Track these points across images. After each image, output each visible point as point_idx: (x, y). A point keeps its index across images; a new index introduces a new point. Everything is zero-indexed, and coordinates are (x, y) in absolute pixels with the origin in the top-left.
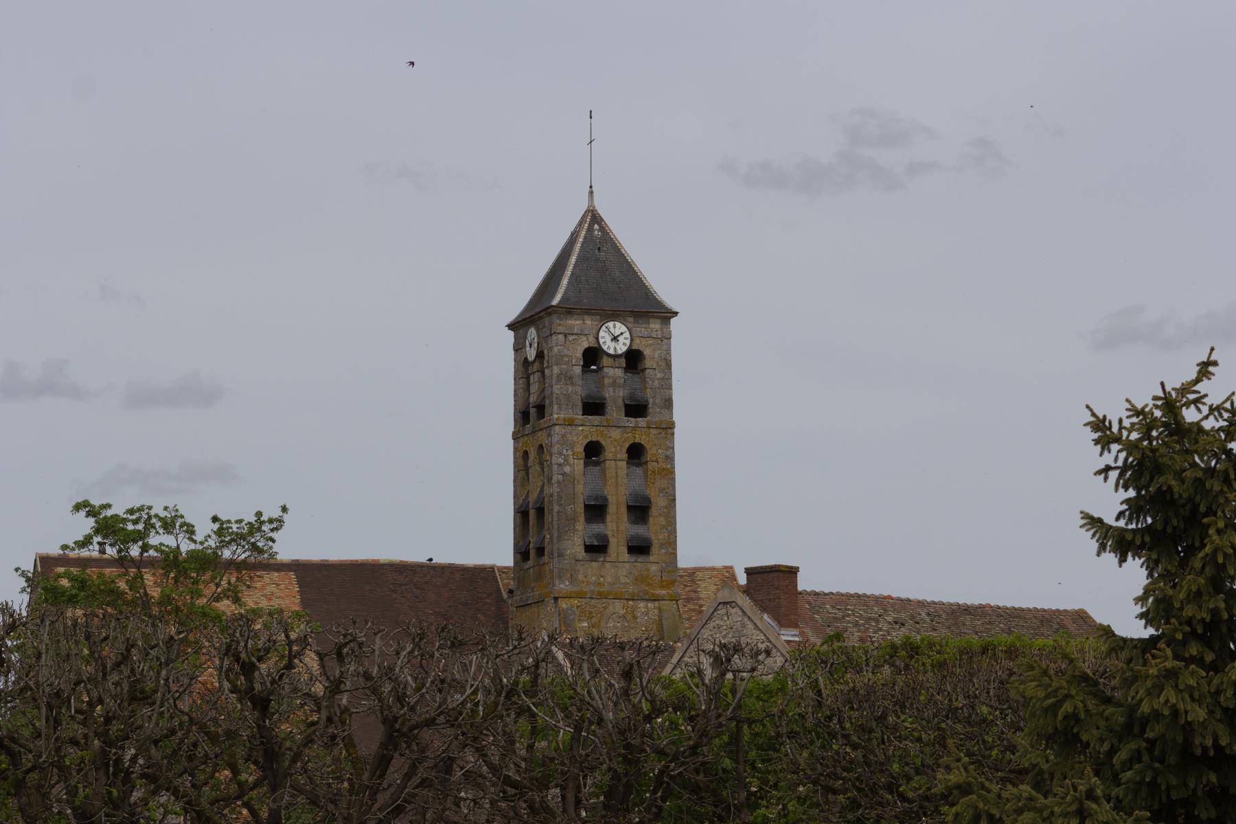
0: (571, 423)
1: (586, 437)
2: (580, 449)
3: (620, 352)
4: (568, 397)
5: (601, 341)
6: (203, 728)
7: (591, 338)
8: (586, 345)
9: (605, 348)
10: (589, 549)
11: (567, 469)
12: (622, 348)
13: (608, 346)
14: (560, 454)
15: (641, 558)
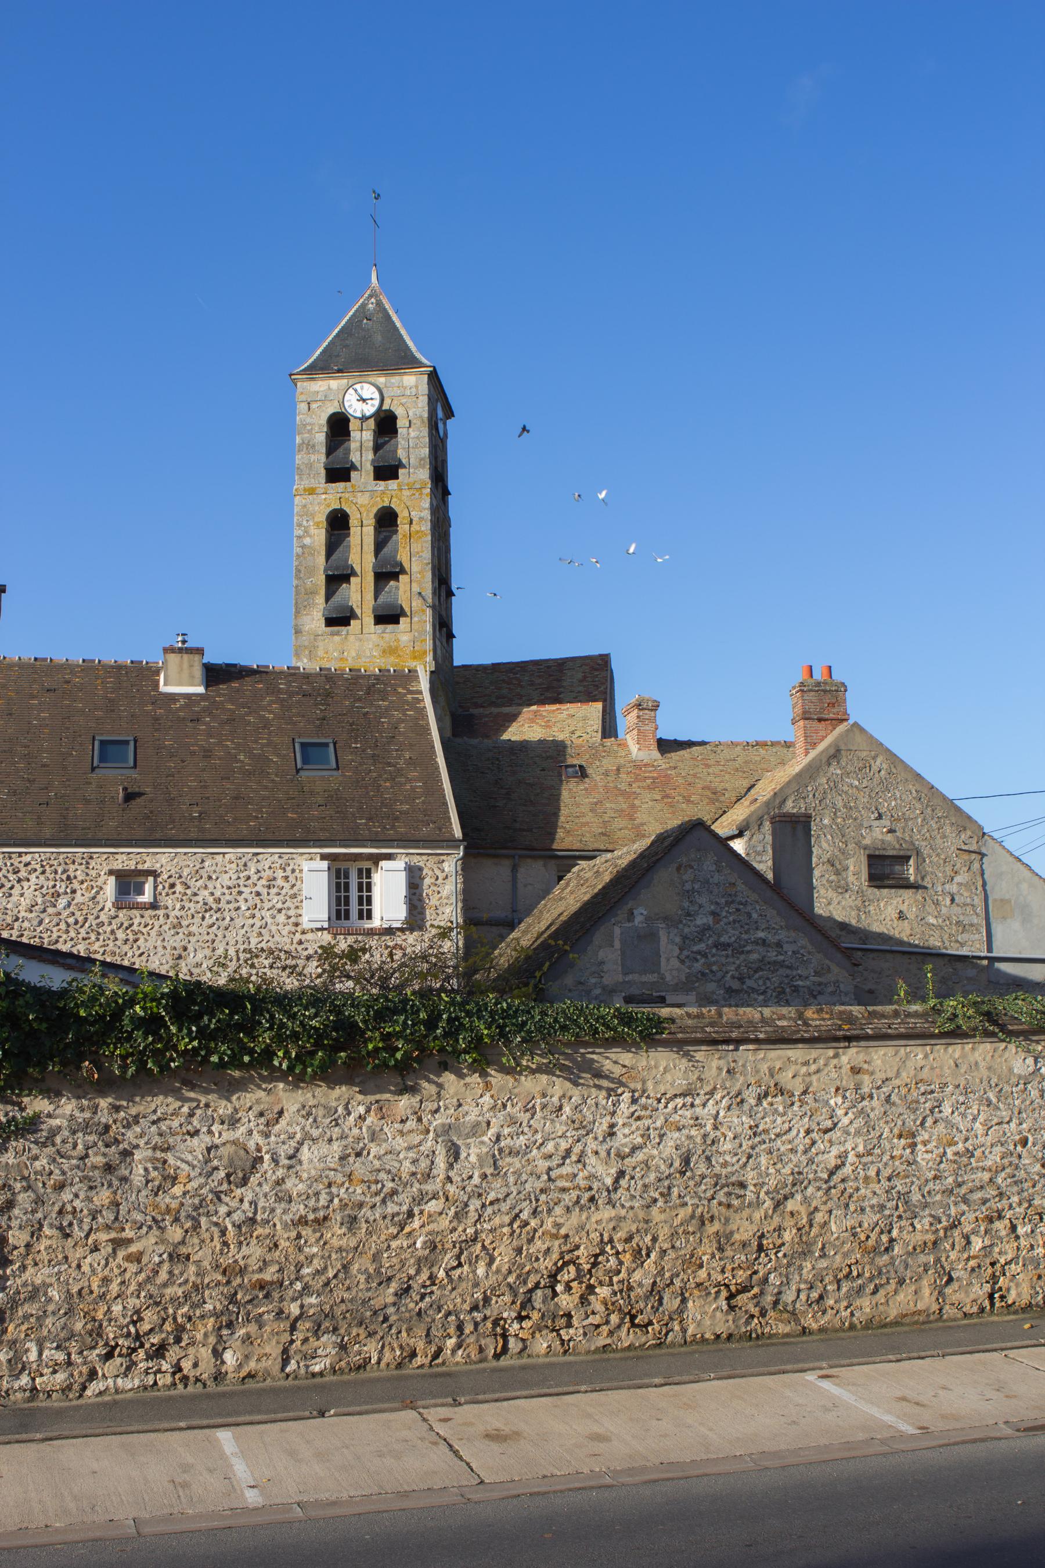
0: (312, 491)
1: (328, 505)
2: (322, 518)
3: (368, 414)
4: (310, 466)
5: (347, 404)
6: (98, 893)
7: (336, 404)
8: (331, 410)
9: (351, 411)
10: (330, 622)
11: (307, 541)
12: (370, 409)
13: (355, 408)
14: (300, 525)
15: (390, 627)
